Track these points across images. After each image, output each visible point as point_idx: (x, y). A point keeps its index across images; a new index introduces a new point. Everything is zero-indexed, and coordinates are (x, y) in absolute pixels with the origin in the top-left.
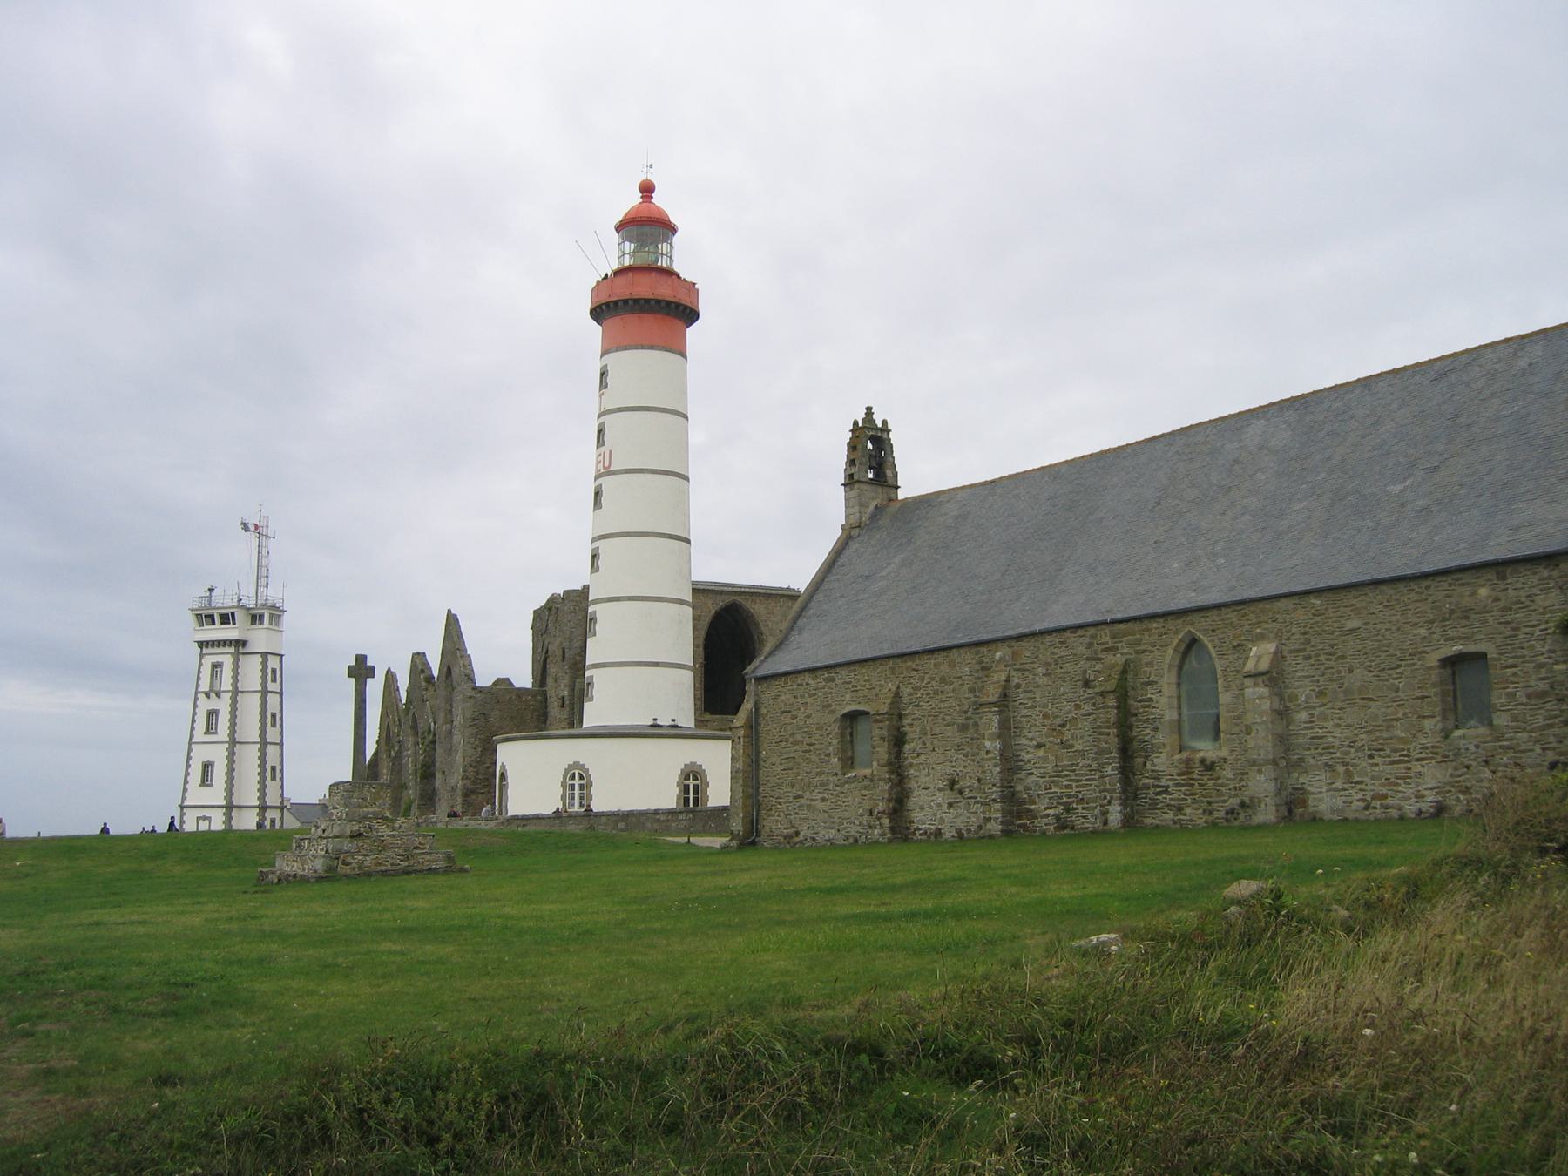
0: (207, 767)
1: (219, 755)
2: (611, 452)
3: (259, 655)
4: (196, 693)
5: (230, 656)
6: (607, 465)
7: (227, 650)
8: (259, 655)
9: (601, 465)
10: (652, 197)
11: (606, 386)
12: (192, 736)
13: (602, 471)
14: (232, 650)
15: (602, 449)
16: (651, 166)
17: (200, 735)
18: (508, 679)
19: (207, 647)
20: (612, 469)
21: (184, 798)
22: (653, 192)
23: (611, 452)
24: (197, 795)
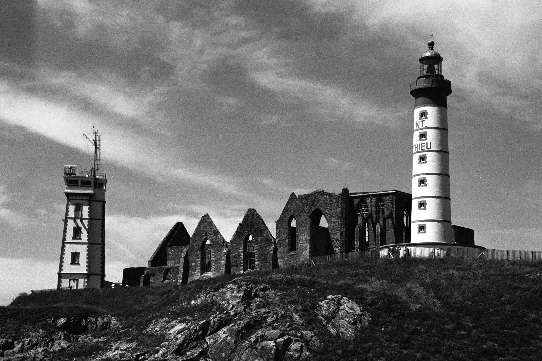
0: (75, 256)
1: (83, 250)
2: (431, 143)
3: (101, 202)
4: (66, 218)
5: (86, 201)
6: (429, 147)
7: (86, 198)
8: (101, 202)
9: (425, 148)
10: (433, 47)
11: (427, 118)
12: (64, 239)
13: (426, 149)
14: (88, 198)
15: (425, 142)
16: (432, 35)
17: (69, 238)
18: (182, 222)
19: (72, 196)
20: (431, 149)
21: (61, 269)
22: (433, 45)
23: (431, 143)
24: (68, 268)
